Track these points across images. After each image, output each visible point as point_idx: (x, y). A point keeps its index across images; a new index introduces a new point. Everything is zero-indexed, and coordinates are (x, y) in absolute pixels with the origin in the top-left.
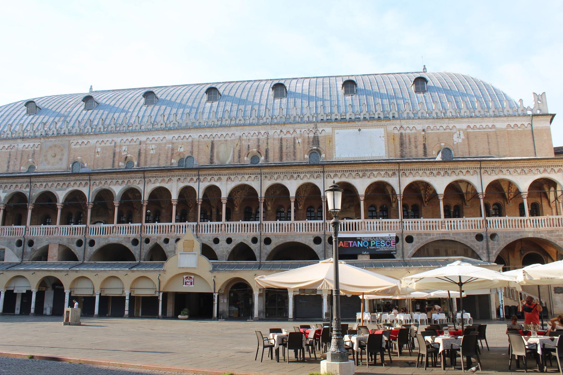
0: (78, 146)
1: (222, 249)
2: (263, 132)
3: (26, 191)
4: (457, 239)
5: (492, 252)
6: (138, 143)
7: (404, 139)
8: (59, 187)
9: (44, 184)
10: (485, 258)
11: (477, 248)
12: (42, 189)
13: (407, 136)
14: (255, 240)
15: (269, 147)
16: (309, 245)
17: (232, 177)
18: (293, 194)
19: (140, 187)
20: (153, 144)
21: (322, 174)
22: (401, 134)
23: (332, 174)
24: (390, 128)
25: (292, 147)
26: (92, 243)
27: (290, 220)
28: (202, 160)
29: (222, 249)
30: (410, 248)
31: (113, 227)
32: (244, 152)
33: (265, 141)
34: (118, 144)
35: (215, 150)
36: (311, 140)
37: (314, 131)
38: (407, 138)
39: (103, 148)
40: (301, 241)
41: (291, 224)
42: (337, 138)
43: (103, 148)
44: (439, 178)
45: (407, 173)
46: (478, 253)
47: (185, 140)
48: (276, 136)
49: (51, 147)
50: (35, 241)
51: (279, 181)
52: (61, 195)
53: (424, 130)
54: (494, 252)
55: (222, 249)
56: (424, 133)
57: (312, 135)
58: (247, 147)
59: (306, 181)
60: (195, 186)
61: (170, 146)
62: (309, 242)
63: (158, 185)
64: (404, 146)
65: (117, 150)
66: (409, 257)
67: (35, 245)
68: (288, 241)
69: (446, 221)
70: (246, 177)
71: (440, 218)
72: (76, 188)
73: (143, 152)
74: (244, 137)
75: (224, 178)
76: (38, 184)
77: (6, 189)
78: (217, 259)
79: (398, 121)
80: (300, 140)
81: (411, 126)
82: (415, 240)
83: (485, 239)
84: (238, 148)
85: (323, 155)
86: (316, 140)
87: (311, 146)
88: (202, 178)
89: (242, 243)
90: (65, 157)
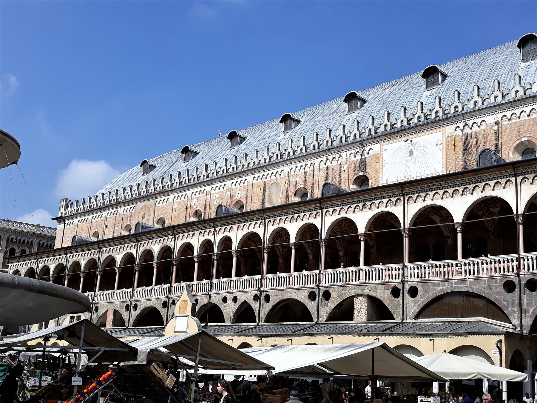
0: (161, 204)
1: (229, 310)
2: (309, 163)
3: (96, 257)
4: (476, 289)
5: (528, 311)
6: (205, 194)
7: (470, 141)
8: (118, 251)
9: (108, 249)
10: (516, 321)
11: (505, 303)
12: (107, 254)
13: (474, 136)
14: (256, 298)
15: (314, 181)
16: (304, 303)
17: (242, 225)
18: (293, 240)
19: (171, 244)
20: (217, 193)
21: (320, 211)
22: (466, 135)
23: (331, 210)
24: (450, 129)
25: (338, 177)
26: (136, 307)
27: (290, 272)
28: (256, 206)
29: (229, 310)
30: (413, 306)
31: (151, 289)
32: (292, 191)
33: (312, 174)
34: (190, 197)
35: (267, 192)
36: (358, 164)
37: (360, 152)
38: (474, 140)
39: (179, 204)
40: (296, 298)
41: (289, 277)
42: (385, 156)
43: (179, 204)
44: (457, 198)
45: (414, 196)
46: (506, 312)
47: (242, 184)
48: (322, 166)
49: (142, 208)
50: (99, 307)
51: (282, 225)
52: (119, 258)
53: (496, 123)
54: (531, 310)
55: (228, 310)
56: (496, 127)
57: (358, 157)
58: (295, 183)
59: (306, 221)
60: (211, 237)
61: (229, 193)
62: (302, 297)
63: (185, 241)
64: (470, 152)
65: (189, 205)
66: (410, 318)
67: (99, 311)
68: (285, 298)
69: (463, 264)
70: (253, 223)
71: (456, 258)
72: (129, 250)
73: (208, 203)
74: (292, 173)
75: (235, 227)
76: (105, 249)
77: (86, 256)
78: (224, 322)
79: (461, 117)
80: (345, 167)
81: (479, 121)
82: (420, 293)
83: (517, 289)
84: (286, 187)
85: (370, 182)
86: (363, 164)
87: (357, 172)
88: (218, 229)
89: (245, 302)
90: (152, 216)
